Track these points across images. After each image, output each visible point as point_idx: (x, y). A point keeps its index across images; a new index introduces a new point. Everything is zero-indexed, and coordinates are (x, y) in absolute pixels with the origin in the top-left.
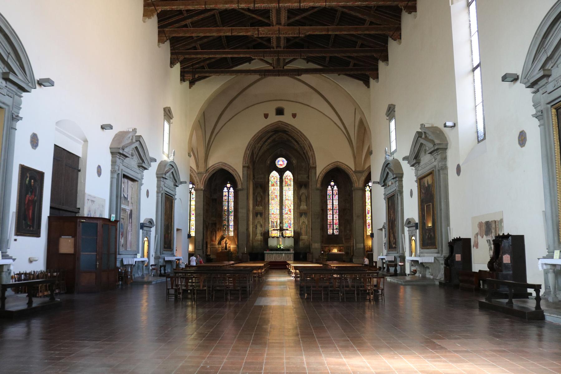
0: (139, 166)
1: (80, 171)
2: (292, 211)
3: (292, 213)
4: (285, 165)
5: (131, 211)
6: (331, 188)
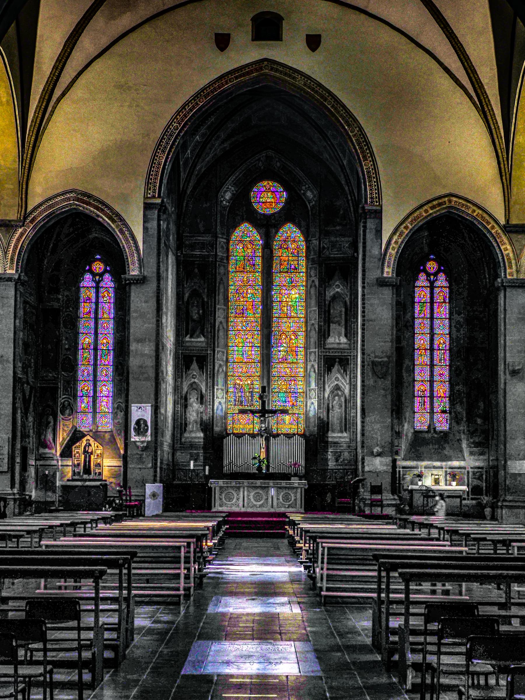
4: (280, 206)
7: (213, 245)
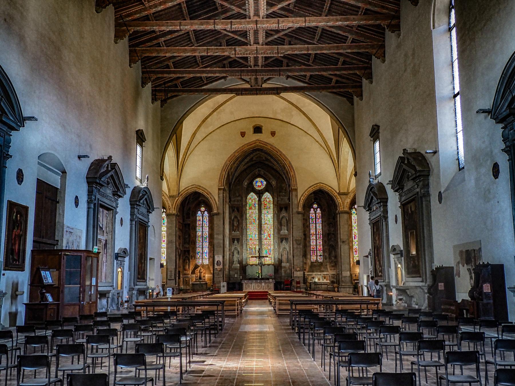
0: (114, 195)
1: (58, 202)
2: (272, 236)
3: (272, 238)
4: (264, 186)
5: (106, 240)
7: (241, 200)
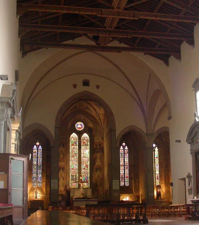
2: (89, 166)
3: (89, 168)
4: (83, 128)
6: (123, 148)
